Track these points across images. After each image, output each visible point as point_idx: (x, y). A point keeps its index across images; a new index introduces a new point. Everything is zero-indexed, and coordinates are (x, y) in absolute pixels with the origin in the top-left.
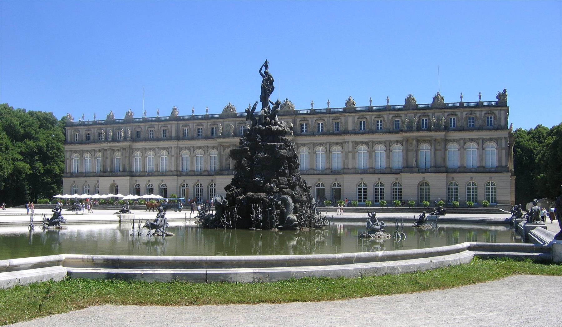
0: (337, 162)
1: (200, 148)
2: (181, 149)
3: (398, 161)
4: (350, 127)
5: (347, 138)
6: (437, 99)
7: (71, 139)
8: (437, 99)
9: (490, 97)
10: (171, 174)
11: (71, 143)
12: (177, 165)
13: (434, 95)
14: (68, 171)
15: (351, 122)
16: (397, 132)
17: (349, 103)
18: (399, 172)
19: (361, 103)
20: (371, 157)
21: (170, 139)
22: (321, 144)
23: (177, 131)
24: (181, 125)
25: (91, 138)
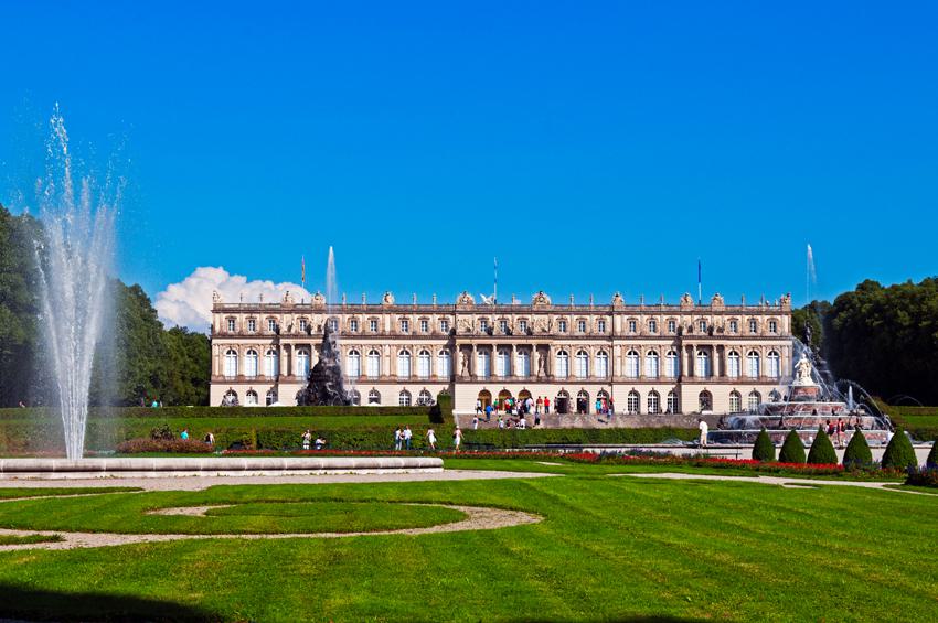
0: (599, 369)
4: (618, 329)
5: (615, 342)
7: (221, 327)
10: (386, 379)
11: (224, 336)
14: (217, 374)
21: (383, 336)
23: (392, 323)
25: (258, 328)
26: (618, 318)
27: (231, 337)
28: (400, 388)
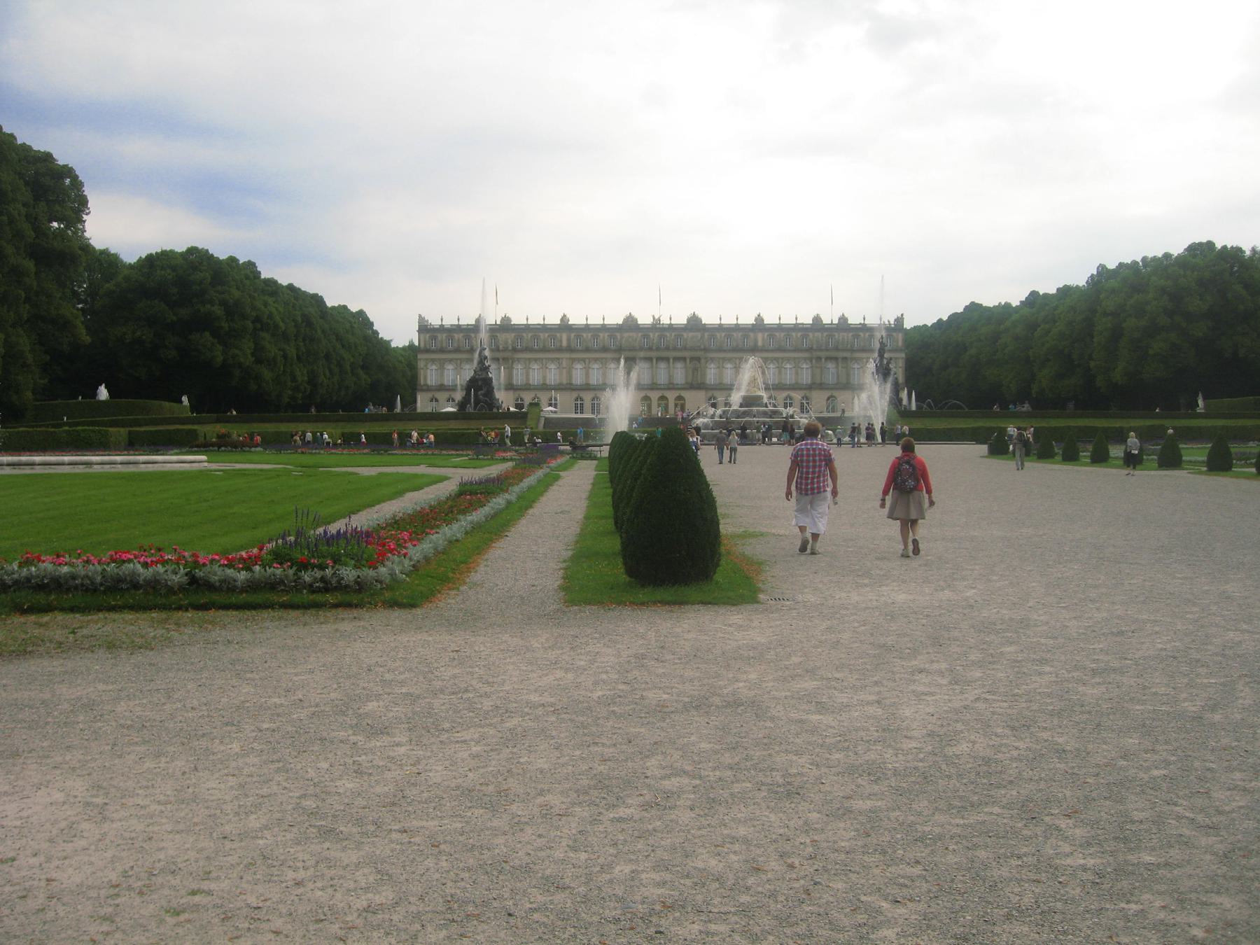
1: (596, 360)
2: (573, 360)
3: (806, 378)
4: (760, 344)
6: (843, 319)
8: (843, 319)
9: (890, 318)
11: (427, 351)
12: (570, 377)
13: (840, 314)
15: (760, 338)
16: (806, 350)
17: (759, 319)
18: (810, 388)
19: (770, 319)
20: (780, 372)
21: (560, 350)
22: (730, 360)
23: (569, 340)
24: (573, 335)
26: (760, 336)
27: (433, 352)
28: (575, 395)
